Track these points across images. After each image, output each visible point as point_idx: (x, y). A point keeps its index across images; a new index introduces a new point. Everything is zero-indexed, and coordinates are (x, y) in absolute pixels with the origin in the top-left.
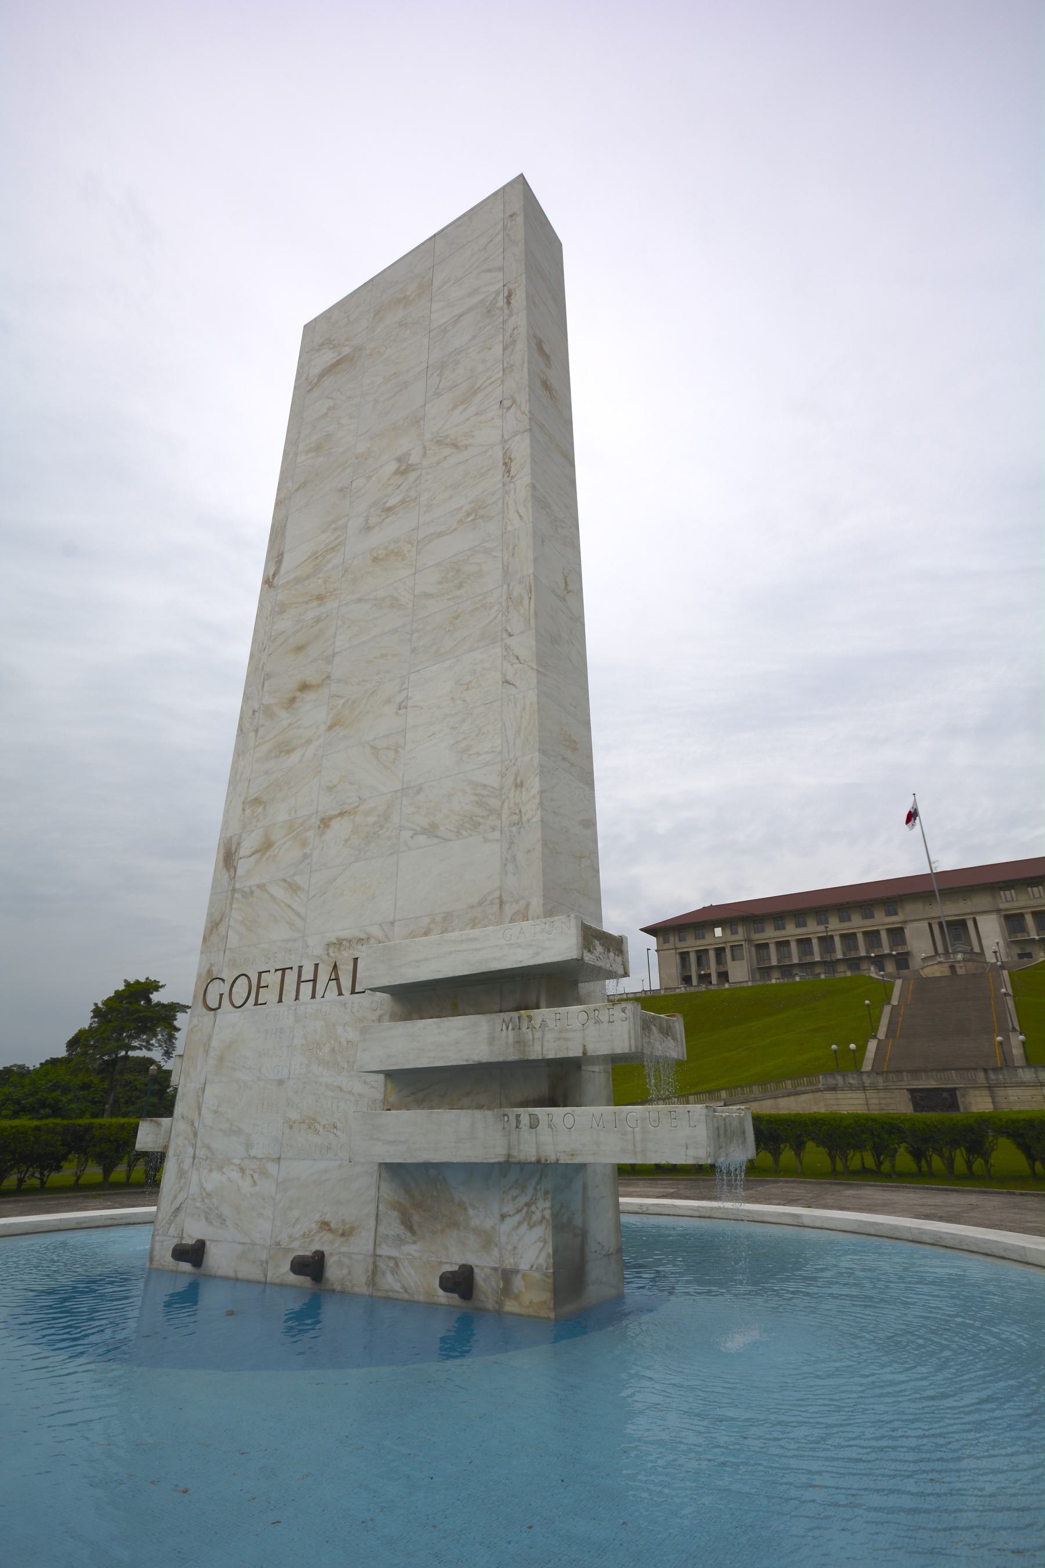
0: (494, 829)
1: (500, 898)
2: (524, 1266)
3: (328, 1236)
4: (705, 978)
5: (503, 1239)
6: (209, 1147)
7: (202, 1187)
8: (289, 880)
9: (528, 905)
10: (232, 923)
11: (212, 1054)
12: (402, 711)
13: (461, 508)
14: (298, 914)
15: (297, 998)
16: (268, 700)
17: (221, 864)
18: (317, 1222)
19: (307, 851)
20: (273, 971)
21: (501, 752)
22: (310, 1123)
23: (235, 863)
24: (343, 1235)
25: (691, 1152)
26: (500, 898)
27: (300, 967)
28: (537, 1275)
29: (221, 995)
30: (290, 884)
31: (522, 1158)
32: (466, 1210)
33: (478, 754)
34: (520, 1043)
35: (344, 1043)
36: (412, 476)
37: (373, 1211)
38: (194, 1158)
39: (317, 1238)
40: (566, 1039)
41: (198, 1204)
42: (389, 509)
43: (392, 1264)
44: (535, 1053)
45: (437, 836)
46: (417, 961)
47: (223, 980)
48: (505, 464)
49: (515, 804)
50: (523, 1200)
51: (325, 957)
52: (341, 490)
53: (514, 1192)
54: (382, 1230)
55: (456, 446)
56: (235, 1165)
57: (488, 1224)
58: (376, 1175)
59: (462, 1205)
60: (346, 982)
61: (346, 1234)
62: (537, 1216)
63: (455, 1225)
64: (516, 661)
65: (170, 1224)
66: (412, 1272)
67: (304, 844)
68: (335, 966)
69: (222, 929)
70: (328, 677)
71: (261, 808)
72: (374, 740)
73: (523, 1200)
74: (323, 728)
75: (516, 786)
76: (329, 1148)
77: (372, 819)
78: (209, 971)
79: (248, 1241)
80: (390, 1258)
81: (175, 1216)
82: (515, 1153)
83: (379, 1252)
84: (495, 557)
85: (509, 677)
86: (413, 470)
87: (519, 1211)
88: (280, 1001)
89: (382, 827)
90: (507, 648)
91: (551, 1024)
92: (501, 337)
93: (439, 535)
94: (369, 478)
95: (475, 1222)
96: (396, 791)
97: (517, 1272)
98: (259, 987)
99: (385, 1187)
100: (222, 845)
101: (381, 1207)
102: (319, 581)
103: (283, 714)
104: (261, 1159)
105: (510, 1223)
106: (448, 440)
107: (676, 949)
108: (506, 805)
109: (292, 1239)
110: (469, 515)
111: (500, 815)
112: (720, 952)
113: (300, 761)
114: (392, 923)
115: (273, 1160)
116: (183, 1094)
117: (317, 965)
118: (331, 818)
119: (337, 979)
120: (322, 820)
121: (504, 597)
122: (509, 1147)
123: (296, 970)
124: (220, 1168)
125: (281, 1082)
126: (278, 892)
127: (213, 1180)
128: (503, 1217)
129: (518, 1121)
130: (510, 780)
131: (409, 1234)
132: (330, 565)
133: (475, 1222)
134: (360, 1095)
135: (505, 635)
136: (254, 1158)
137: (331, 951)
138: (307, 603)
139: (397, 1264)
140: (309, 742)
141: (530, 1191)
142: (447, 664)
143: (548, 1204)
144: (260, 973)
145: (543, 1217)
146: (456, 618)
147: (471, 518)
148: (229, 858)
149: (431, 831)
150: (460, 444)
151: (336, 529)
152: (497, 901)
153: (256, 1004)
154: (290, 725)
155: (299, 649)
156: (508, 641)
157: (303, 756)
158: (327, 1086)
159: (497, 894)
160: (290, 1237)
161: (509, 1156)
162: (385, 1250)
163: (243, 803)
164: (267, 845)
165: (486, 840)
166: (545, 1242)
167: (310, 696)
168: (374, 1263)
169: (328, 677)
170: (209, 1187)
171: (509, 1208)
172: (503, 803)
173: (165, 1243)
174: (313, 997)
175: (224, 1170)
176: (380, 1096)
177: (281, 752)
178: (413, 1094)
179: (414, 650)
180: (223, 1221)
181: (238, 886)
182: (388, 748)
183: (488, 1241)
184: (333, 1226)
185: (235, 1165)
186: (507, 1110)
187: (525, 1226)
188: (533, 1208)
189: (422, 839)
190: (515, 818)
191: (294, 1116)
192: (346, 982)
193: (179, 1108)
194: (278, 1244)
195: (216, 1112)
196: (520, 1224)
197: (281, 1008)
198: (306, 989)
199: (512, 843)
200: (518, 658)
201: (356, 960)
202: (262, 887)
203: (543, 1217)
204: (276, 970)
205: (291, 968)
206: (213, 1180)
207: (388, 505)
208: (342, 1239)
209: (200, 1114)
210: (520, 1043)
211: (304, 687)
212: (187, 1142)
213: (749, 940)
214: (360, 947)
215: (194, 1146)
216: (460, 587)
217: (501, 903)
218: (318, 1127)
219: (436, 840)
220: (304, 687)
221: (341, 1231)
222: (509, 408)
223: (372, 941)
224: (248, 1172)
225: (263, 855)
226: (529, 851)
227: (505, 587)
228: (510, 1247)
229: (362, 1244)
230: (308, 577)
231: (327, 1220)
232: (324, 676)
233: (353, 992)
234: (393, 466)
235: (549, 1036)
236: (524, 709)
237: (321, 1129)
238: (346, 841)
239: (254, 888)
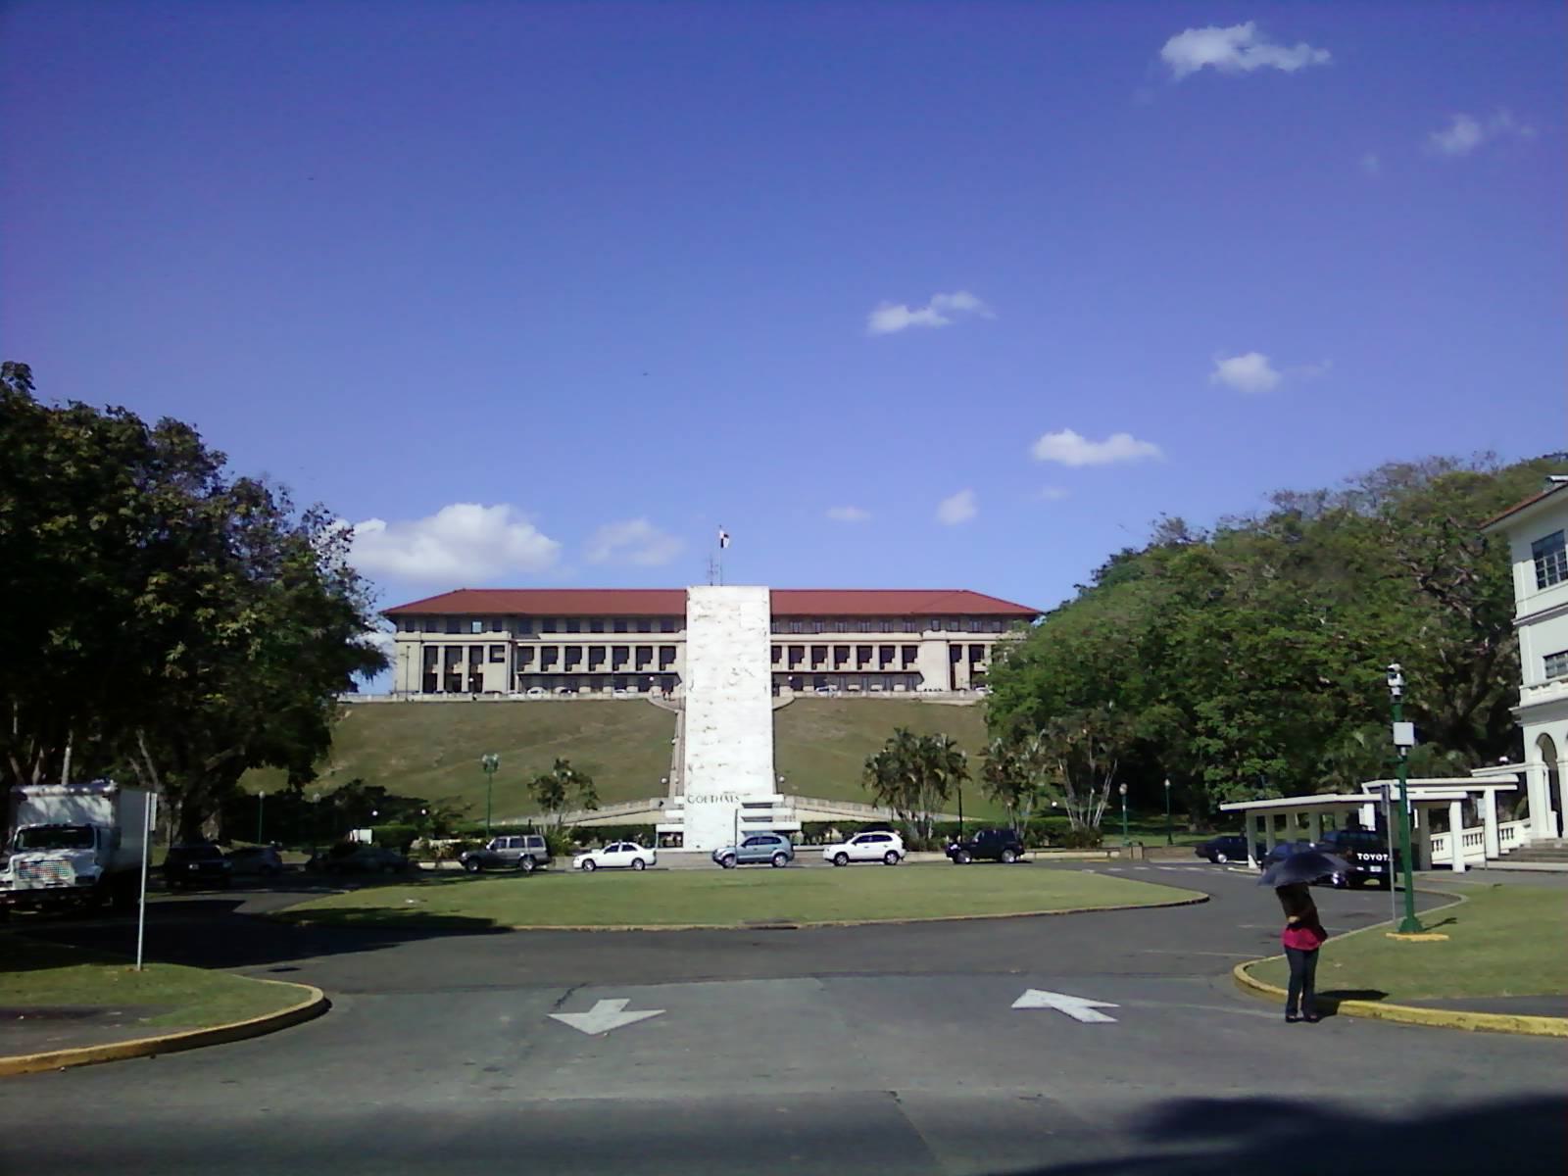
4: (453, 685)
60: (729, 799)
107: (422, 642)
112: (476, 650)
149: (748, 773)
164: (702, 767)
193: (685, 822)
211: (708, 728)
213: (513, 643)
220: (708, 728)
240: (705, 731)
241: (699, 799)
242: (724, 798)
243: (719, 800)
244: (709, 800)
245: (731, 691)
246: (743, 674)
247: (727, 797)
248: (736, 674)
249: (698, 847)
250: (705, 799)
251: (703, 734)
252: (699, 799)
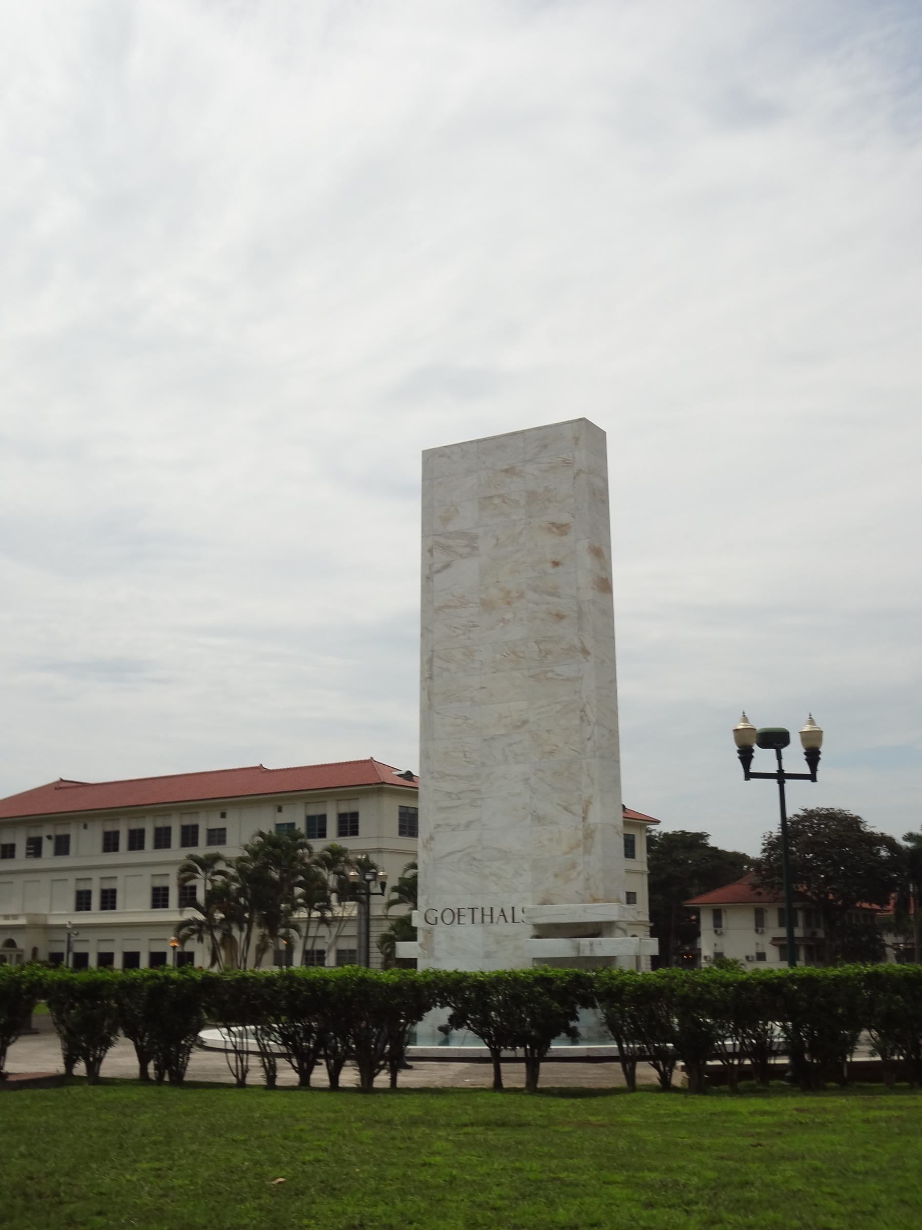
15: (483, 922)
68: (502, 911)
123: (480, 910)
192: (509, 919)
233: (513, 922)
242: (497, 913)
243: (487, 912)
244: (466, 920)
252: (448, 918)
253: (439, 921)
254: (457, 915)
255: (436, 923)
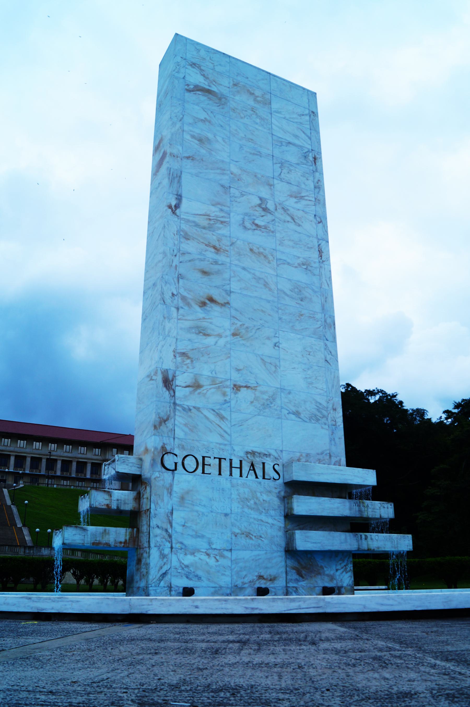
0: (325, 424)
1: (329, 453)
2: (345, 585)
3: (263, 581)
5: (338, 577)
6: (181, 543)
7: (181, 562)
8: (217, 411)
9: (340, 460)
10: (176, 423)
11: (174, 494)
12: (276, 348)
13: (299, 257)
14: (226, 432)
15: (231, 474)
16: (182, 291)
17: (161, 384)
18: (257, 576)
19: (227, 398)
20: (212, 458)
21: (326, 392)
22: (248, 535)
23: (173, 387)
24: (271, 580)
25: (409, 547)
26: (329, 453)
27: (231, 460)
28: (349, 587)
29: (176, 464)
30: (217, 413)
31: (363, 548)
32: (323, 568)
33: (317, 388)
34: (360, 511)
35: (262, 501)
36: (269, 217)
37: (283, 570)
38: (172, 548)
39: (257, 582)
40: (375, 512)
41: (179, 571)
42: (257, 225)
43: (295, 589)
44: (365, 515)
45: (300, 418)
46: (319, 474)
47: (176, 455)
48: (319, 251)
49: (334, 417)
50: (343, 565)
51: (246, 458)
52: (223, 186)
53: (340, 562)
54: (289, 577)
55: (293, 219)
56: (203, 552)
57: (332, 573)
58: (284, 557)
59: (322, 567)
60: (260, 473)
61: (273, 579)
62: (348, 569)
63: (320, 574)
64: (330, 353)
65: (160, 581)
66: (304, 591)
67: (224, 394)
68: (252, 465)
69: (170, 424)
70: (228, 303)
71: (188, 361)
72: (262, 355)
73: (343, 565)
74: (228, 333)
75: (333, 409)
76: (259, 545)
77: (266, 397)
78: (163, 448)
79: (217, 586)
80: (293, 587)
81: (163, 577)
82: (360, 547)
83: (288, 585)
84: (317, 296)
85: (328, 359)
86: (270, 213)
87: (342, 568)
88: (220, 474)
89: (271, 403)
90: (326, 345)
91: (370, 506)
92: (311, 178)
93: (289, 264)
94: (242, 195)
95: (327, 572)
96: (278, 388)
97: (342, 587)
98: (204, 465)
99: (289, 562)
100: (159, 372)
101: (288, 569)
102: (215, 237)
103: (198, 308)
104: (220, 550)
105: (338, 573)
106: (289, 212)
108: (330, 415)
109: (244, 583)
110: (303, 264)
111: (327, 419)
113: (215, 344)
114: (282, 451)
115: (227, 550)
116: (155, 514)
117: (241, 462)
118: (240, 387)
119: (254, 470)
120: (235, 385)
121: (323, 320)
122: (359, 545)
124: (193, 554)
125: (226, 515)
126: (211, 416)
127: (188, 560)
128: (337, 570)
129: (361, 537)
130: (331, 406)
131: (301, 578)
132: (220, 232)
133: (327, 572)
134: (273, 524)
135: (324, 338)
136: (215, 549)
137: (249, 456)
138: (206, 245)
139: (297, 589)
140: (220, 336)
141: (346, 561)
142: (299, 336)
143: (352, 565)
144: (204, 458)
145: (350, 570)
146: (302, 315)
147: (305, 267)
148: (168, 383)
149: (297, 414)
150: (295, 220)
151: (221, 210)
152: (328, 455)
153: (203, 472)
154: (204, 318)
155: (205, 273)
156: (326, 342)
157: (216, 342)
158: (254, 519)
159: (328, 452)
160: (242, 583)
161: (359, 548)
162: (291, 585)
163: (174, 351)
165: (322, 428)
166: (351, 577)
167: (216, 308)
168: (287, 590)
169: (228, 303)
170: (186, 562)
171: (339, 567)
172: (328, 414)
173: (158, 591)
174: (241, 476)
175: (195, 554)
176: (282, 525)
177: (200, 332)
178: (298, 526)
179: (280, 319)
180: (199, 578)
181: (178, 402)
182: (270, 363)
183: (332, 578)
184: (265, 577)
185: (203, 552)
186: (357, 533)
187: (344, 573)
188: (347, 567)
189: (293, 417)
190: (334, 423)
191: (237, 531)
192: (260, 473)
194: (236, 586)
195: (184, 526)
196: (343, 572)
197: (219, 478)
198: (236, 472)
199: (333, 433)
200: (331, 352)
201: (264, 464)
202: (198, 409)
203: (350, 570)
204: (215, 458)
205: (225, 459)
206: (188, 560)
207: (256, 222)
208: (271, 582)
209: (171, 526)
210: (360, 511)
212: (164, 540)
214: (265, 458)
215: (171, 542)
216: (302, 300)
217: (330, 456)
218: (252, 536)
219: (300, 420)
220: (211, 300)
221: (269, 579)
222: (319, 223)
223: (272, 457)
224: (212, 555)
225: (195, 390)
226: (340, 438)
227: (323, 315)
228: (340, 580)
229: (281, 583)
230: (204, 228)
231: (262, 574)
232: (226, 302)
234: (259, 202)
235: (370, 510)
236: (334, 377)
237: (253, 538)
238: (252, 402)
239: (191, 408)
240: (203, 304)
241: (190, 463)
242: (246, 468)
243: (236, 463)
245: (257, 239)
246: (279, 214)
247: (253, 465)
248: (265, 210)
249: (188, 592)
250: (202, 464)
251: (200, 312)
252: (190, 463)
253: (180, 467)
254: (202, 464)
255: (176, 469)
